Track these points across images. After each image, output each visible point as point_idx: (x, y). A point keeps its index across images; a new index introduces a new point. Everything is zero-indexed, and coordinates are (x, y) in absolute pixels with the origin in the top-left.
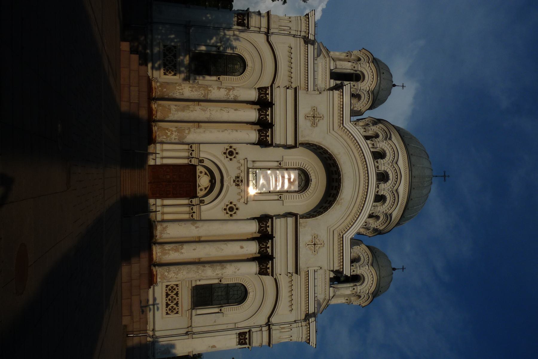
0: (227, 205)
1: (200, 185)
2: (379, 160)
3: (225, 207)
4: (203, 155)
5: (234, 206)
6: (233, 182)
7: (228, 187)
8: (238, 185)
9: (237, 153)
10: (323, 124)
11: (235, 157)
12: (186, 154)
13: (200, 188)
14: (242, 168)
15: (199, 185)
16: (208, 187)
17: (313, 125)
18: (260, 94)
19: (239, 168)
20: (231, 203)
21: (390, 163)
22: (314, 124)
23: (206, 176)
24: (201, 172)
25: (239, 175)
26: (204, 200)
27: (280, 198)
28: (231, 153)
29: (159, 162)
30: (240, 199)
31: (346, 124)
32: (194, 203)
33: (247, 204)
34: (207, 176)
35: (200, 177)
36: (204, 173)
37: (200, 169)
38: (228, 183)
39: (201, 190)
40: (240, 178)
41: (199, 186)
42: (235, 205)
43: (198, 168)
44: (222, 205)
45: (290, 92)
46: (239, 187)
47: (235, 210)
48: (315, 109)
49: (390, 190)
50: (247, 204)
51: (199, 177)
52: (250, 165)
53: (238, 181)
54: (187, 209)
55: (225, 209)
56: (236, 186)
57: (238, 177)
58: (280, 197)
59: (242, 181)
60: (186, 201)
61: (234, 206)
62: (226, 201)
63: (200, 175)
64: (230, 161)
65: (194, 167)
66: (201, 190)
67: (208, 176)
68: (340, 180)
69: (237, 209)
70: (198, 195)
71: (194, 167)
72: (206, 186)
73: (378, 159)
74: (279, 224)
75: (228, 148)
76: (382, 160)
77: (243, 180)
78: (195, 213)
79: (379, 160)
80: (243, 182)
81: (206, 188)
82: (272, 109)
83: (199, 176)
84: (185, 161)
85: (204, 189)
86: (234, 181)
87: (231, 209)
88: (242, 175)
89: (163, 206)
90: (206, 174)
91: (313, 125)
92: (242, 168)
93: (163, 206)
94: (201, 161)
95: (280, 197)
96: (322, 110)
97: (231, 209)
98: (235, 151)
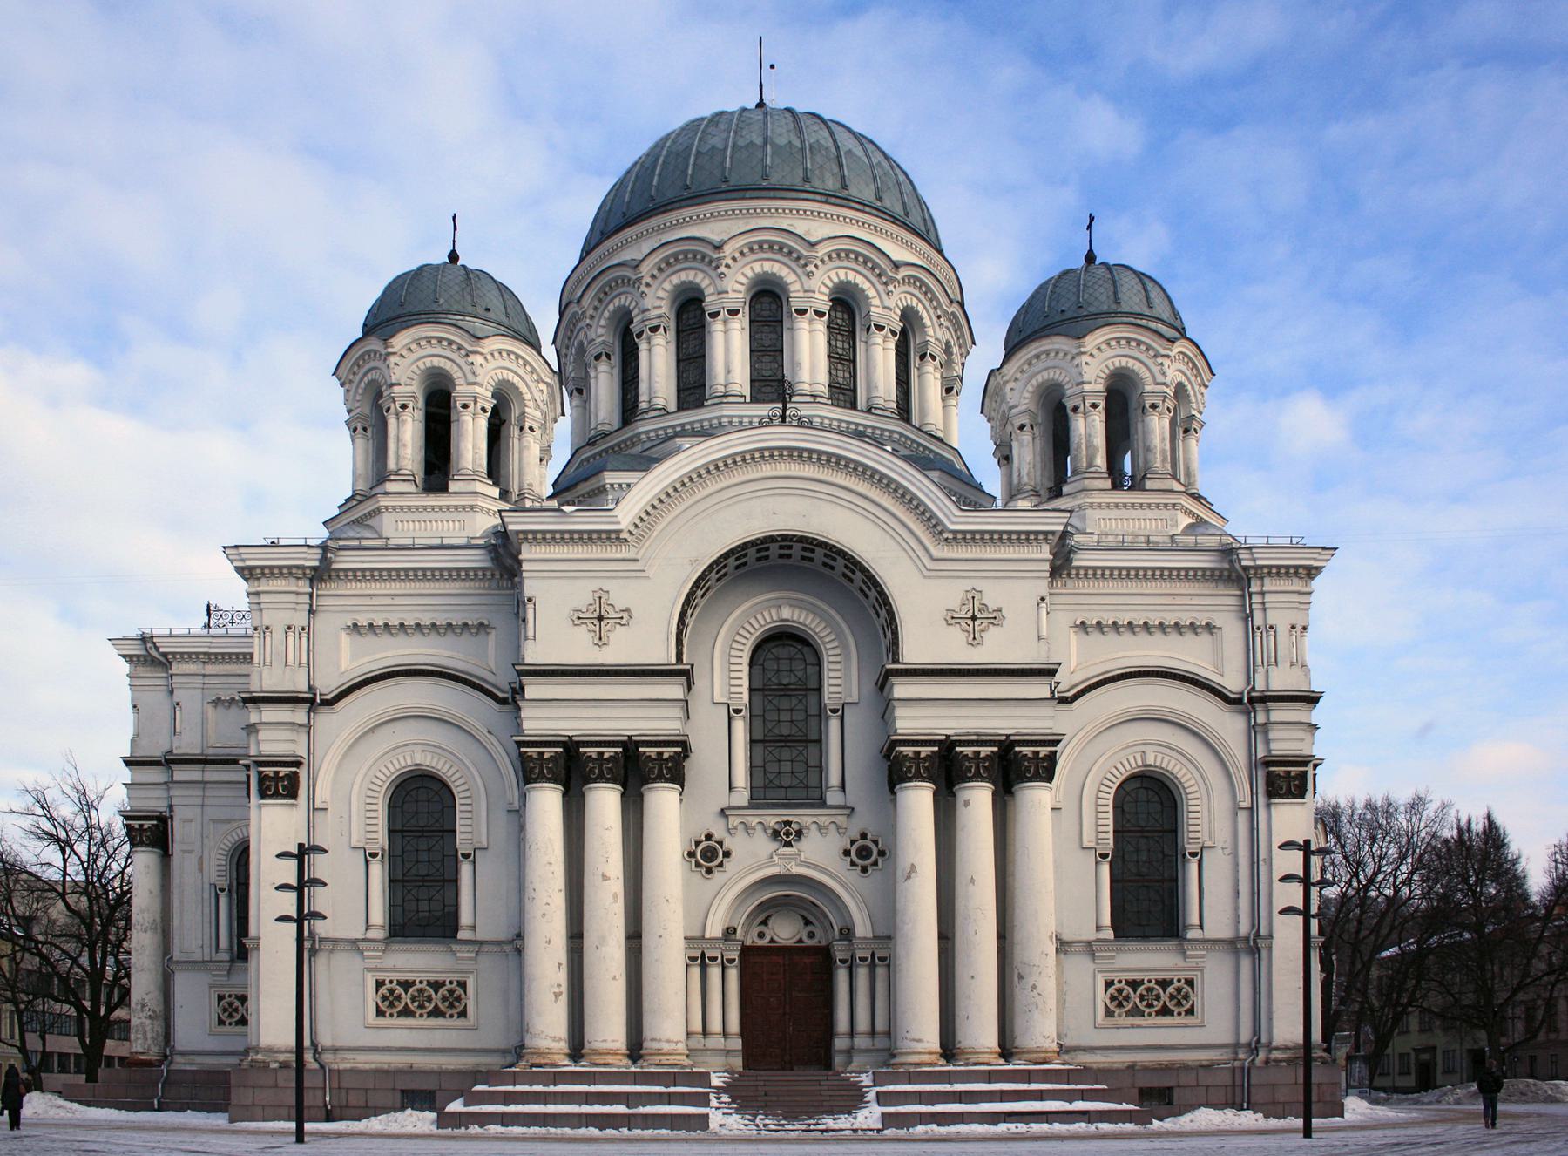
0: (853, 864)
1: (798, 938)
2: (709, 309)
4: (715, 930)
5: (856, 845)
6: (790, 849)
8: (799, 834)
9: (709, 837)
10: (621, 594)
11: (721, 843)
12: (715, 972)
13: (805, 938)
14: (754, 821)
15: (797, 942)
16: (804, 917)
17: (623, 622)
18: (541, 778)
19: (748, 829)
20: (847, 853)
21: (719, 271)
22: (622, 618)
23: (771, 922)
24: (761, 935)
25: (770, 831)
26: (841, 930)
27: (838, 710)
28: (709, 854)
29: (737, 1043)
30: (838, 828)
31: (619, 523)
32: (847, 956)
33: (853, 809)
34: (773, 918)
35: (776, 938)
36: (762, 928)
37: (752, 939)
38: (793, 863)
40: (777, 827)
41: (801, 941)
42: (853, 842)
43: (749, 943)
44: (854, 876)
45: (534, 689)
46: (804, 831)
47: (868, 843)
48: (576, 615)
49: (814, 269)
50: (853, 809)
51: (775, 942)
52: (742, 797)
53: (788, 834)
54: (862, 973)
55: (864, 870)
56: (803, 838)
57: (776, 834)
58: (832, 711)
59: (788, 823)
60: (842, 976)
61: (856, 845)
62: (840, 866)
63: (768, 938)
64: (732, 857)
65: (746, 951)
66: (811, 935)
67: (770, 916)
68: (785, 538)
69: (864, 836)
70: (824, 943)
71: (746, 951)
72: (802, 922)
73: (703, 312)
74: (908, 723)
75: (693, 862)
76: (707, 299)
77: (785, 819)
78: (876, 951)
79: (706, 309)
80: (789, 819)
81: (807, 923)
82: (583, 742)
83: (772, 941)
84: (733, 974)
85: (810, 928)
86: (788, 844)
87: (864, 853)
88: (772, 822)
89: (852, 1033)
90: (765, 923)
91: (623, 622)
92: (754, 821)
93: (852, 1033)
94: (729, 932)
95: (834, 711)
96: (580, 594)
97: (864, 853)
98: (701, 842)
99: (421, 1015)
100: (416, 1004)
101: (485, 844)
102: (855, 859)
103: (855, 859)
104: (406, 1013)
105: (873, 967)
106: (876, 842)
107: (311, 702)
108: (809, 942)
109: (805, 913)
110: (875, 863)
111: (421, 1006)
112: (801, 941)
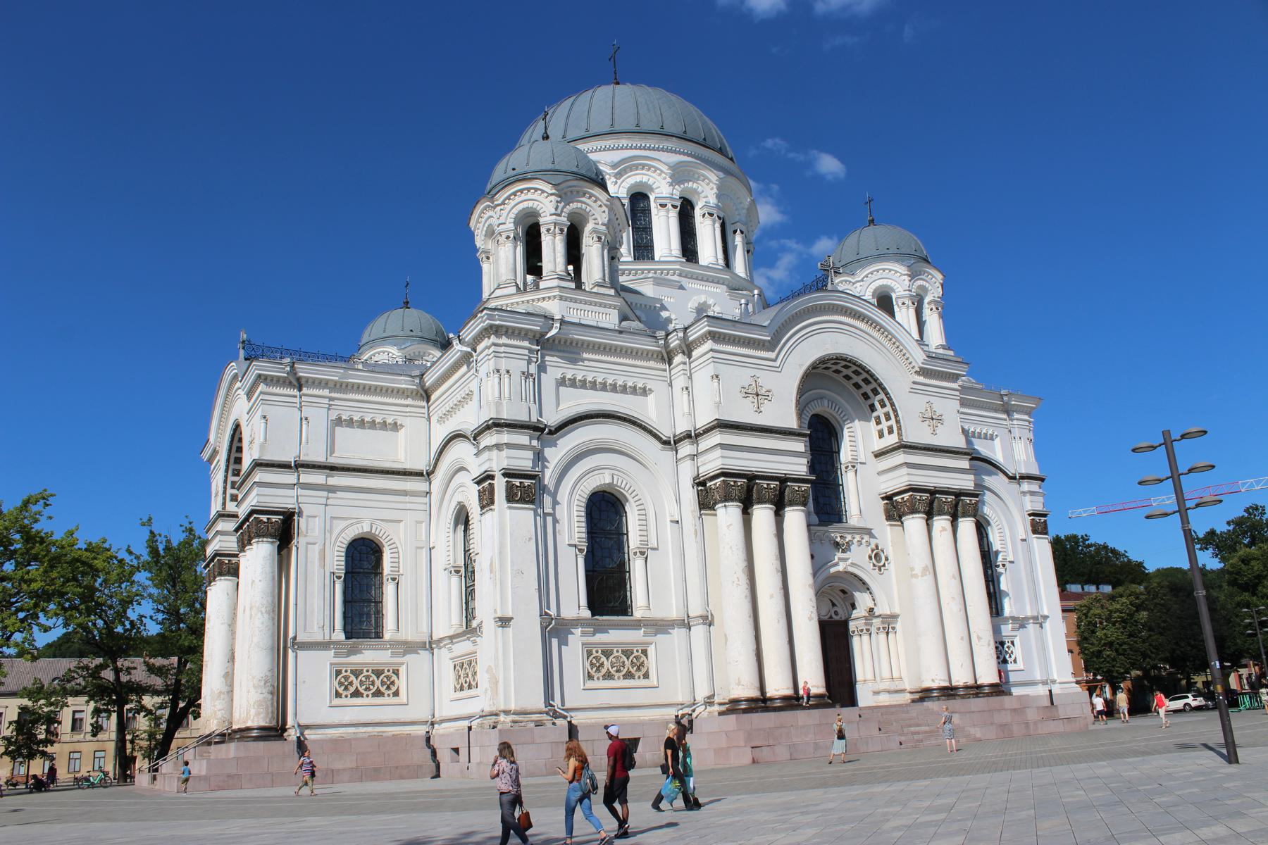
0: (874, 565)
1: (829, 615)
3: (877, 568)
6: (845, 554)
7: (853, 564)
16: (832, 601)
20: (870, 558)
39: (836, 613)
41: (831, 617)
61: (875, 552)
70: (843, 619)
81: (834, 605)
82: (759, 476)
85: (835, 608)
86: (844, 551)
99: (619, 678)
100: (615, 669)
101: (656, 546)
102: (875, 563)
103: (875, 563)
104: (608, 676)
105: (888, 633)
106: (883, 551)
107: (542, 432)
108: (836, 618)
109: (833, 599)
110: (884, 565)
111: (618, 671)
112: (831, 617)
